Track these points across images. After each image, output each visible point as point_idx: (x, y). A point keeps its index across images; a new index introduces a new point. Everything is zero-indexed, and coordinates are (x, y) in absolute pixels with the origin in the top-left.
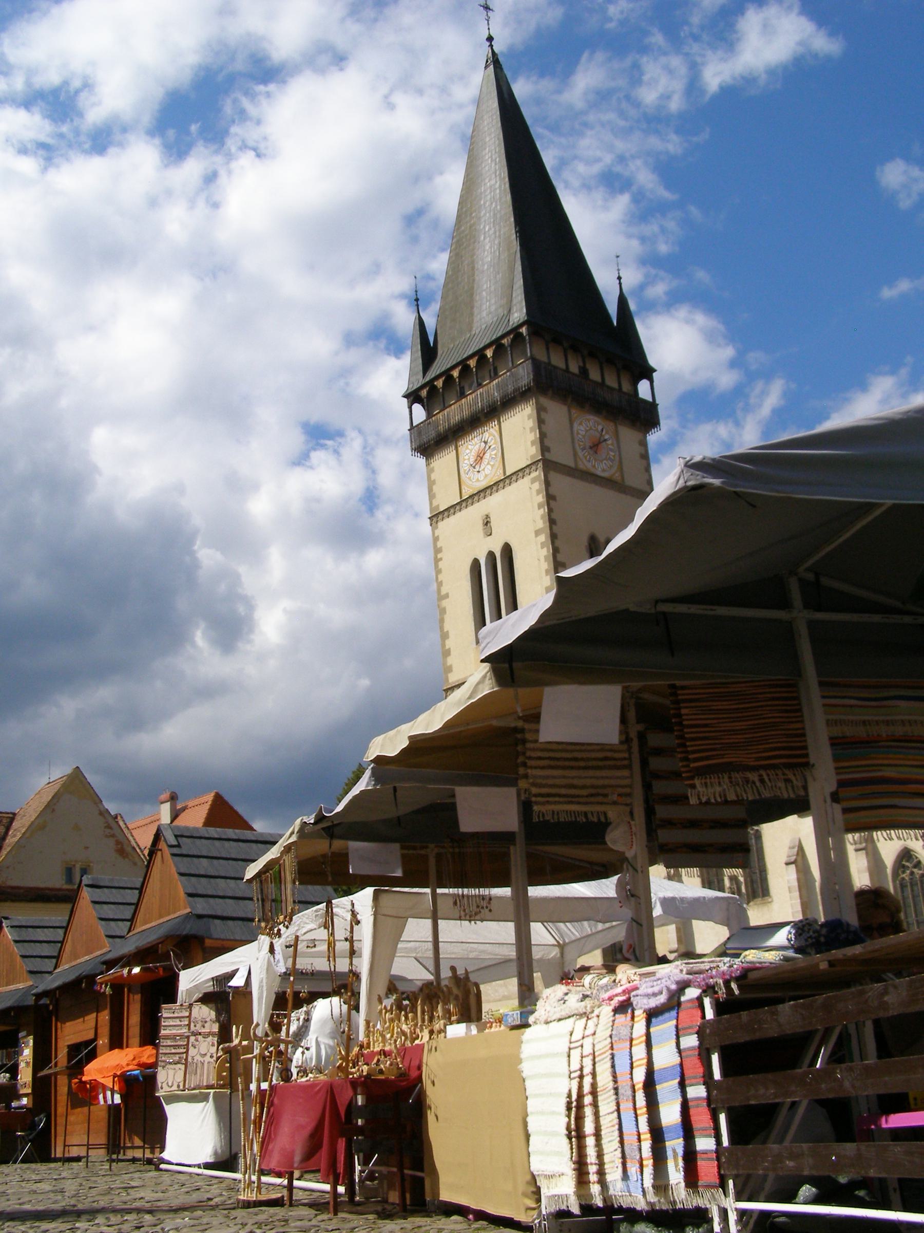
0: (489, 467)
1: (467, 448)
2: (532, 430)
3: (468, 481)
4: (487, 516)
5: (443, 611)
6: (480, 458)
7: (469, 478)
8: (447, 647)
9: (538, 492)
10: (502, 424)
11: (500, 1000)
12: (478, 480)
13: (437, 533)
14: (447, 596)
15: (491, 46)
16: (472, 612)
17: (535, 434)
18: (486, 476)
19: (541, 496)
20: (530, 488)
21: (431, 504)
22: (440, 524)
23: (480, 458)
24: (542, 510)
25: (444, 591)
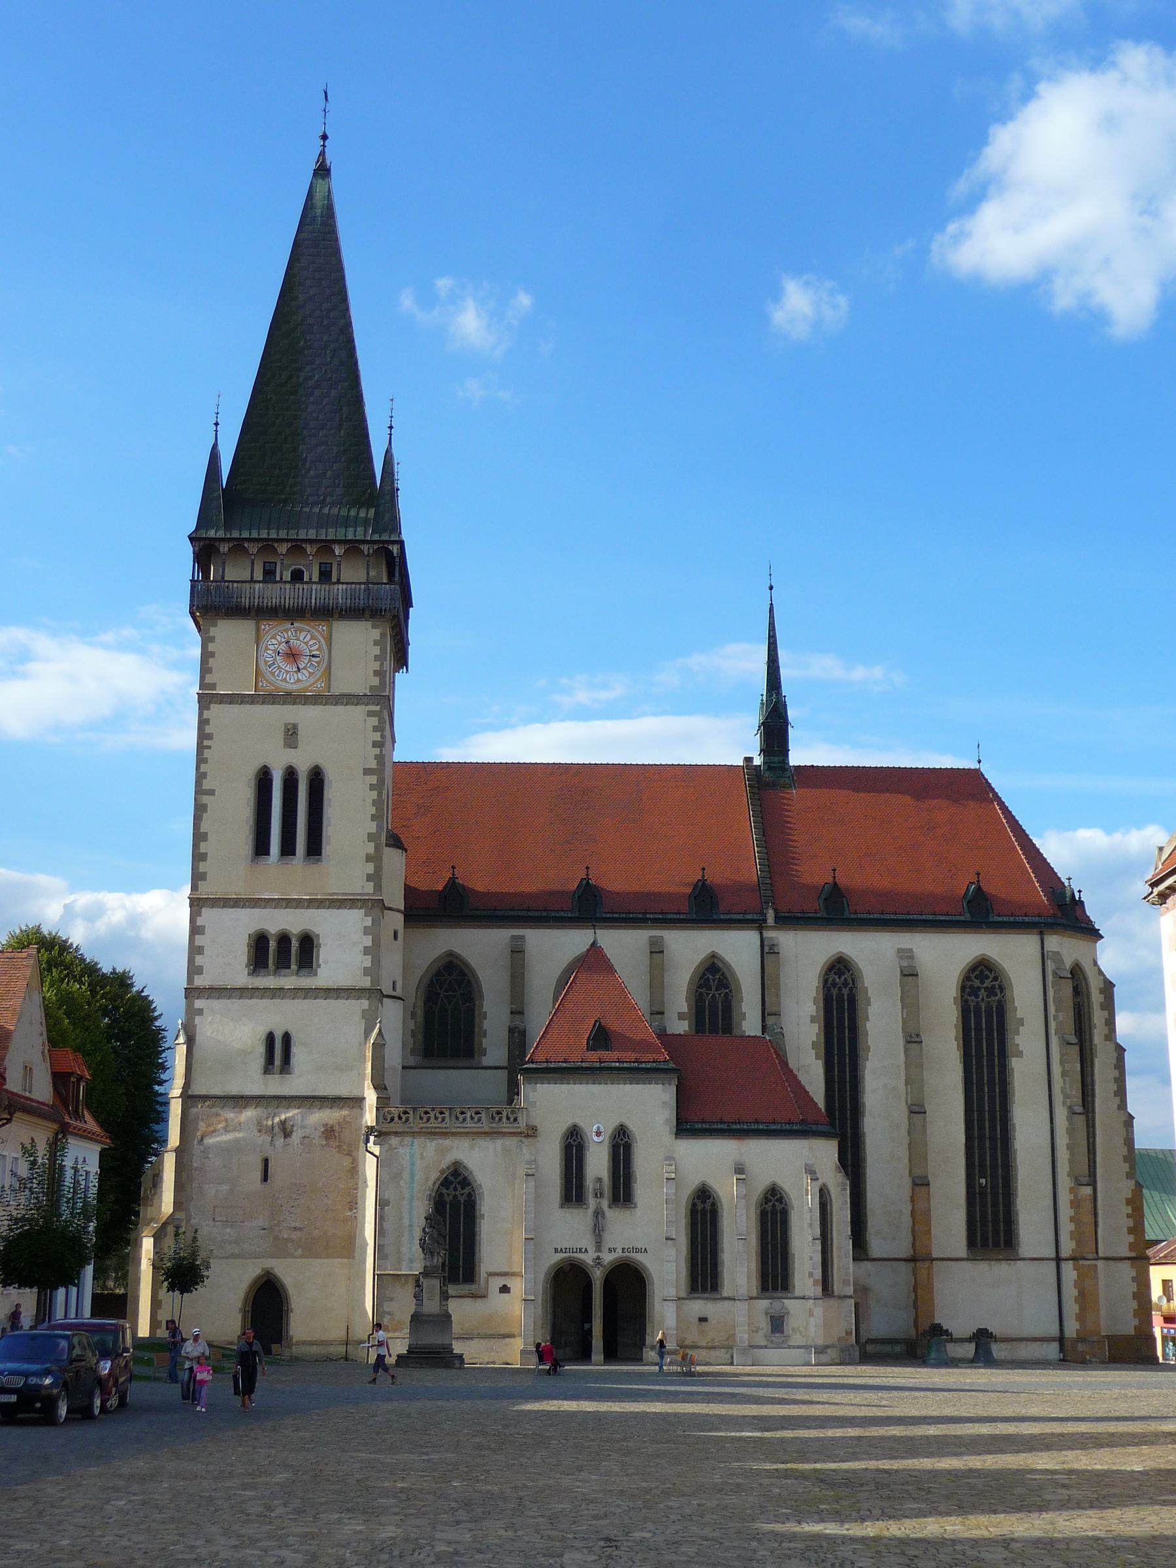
1: (274, 637)
3: (268, 674)
4: (295, 726)
7: (273, 674)
8: (202, 850)
9: (375, 729)
11: (226, 1258)
12: (285, 680)
13: (206, 714)
14: (211, 792)
15: (324, 146)
16: (251, 822)
17: (382, 665)
18: (299, 680)
19: (379, 734)
20: (365, 720)
21: (202, 678)
22: (215, 708)
24: (377, 751)
25: (206, 785)
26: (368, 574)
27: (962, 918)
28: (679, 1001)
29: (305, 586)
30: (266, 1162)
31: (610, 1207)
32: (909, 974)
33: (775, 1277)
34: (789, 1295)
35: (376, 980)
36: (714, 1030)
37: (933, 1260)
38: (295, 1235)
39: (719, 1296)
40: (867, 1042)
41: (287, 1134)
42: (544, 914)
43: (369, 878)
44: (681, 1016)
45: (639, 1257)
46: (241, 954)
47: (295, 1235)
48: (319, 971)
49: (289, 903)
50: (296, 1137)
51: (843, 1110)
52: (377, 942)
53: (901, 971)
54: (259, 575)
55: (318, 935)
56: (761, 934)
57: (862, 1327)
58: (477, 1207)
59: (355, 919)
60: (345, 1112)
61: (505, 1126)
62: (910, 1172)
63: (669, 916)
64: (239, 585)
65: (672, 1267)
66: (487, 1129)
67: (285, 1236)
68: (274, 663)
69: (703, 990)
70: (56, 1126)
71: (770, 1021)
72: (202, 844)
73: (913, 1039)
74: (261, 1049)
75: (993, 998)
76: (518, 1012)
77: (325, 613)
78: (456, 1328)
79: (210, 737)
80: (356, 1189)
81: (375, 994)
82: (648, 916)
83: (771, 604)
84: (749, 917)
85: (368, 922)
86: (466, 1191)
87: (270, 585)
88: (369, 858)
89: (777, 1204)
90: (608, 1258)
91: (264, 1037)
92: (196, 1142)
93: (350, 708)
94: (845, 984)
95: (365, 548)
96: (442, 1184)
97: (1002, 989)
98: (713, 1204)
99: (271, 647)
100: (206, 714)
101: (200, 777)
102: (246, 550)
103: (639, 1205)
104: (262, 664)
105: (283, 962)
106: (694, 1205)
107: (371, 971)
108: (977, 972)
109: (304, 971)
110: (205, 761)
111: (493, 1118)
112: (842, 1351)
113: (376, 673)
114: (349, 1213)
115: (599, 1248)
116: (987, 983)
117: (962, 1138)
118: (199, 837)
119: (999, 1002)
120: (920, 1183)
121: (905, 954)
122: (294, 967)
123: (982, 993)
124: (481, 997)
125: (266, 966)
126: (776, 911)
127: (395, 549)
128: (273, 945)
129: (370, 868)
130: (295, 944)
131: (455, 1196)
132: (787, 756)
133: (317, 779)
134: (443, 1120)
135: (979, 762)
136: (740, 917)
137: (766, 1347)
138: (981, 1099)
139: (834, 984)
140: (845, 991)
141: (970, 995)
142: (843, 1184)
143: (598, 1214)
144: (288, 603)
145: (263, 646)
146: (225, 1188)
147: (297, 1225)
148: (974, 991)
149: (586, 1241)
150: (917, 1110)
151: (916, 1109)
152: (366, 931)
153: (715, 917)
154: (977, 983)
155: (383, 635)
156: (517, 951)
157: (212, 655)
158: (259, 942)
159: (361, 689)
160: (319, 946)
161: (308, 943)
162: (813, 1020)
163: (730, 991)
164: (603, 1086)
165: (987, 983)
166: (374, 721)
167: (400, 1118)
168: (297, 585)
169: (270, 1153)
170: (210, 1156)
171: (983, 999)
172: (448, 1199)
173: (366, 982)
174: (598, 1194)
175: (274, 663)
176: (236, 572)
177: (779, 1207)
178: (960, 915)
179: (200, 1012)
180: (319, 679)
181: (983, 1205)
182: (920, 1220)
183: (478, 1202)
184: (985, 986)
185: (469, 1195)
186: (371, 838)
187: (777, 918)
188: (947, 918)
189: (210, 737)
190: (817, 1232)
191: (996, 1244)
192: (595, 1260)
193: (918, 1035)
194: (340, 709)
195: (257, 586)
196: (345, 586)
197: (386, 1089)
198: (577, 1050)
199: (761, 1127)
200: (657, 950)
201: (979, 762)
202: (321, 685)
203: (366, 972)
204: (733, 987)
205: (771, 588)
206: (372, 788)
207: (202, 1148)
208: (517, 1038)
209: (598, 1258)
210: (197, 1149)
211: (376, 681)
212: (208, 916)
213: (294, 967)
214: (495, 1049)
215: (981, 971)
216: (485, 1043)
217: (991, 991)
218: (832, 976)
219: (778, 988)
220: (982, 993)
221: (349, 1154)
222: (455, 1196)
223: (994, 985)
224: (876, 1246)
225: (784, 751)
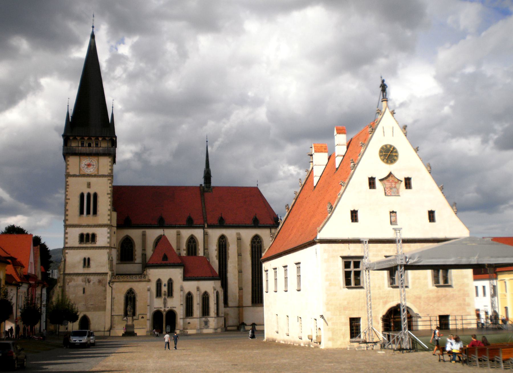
0: (93, 170)
1: (84, 160)
2: (110, 166)
5: (66, 204)
6: (89, 165)
9: (110, 183)
10: (99, 160)
12: (87, 171)
13: (67, 180)
14: (69, 199)
17: (111, 168)
18: (90, 171)
21: (66, 171)
23: (89, 165)
24: (110, 189)
25: (68, 197)
26: (108, 145)
27: (252, 225)
28: (184, 246)
29: (92, 148)
30: (84, 289)
31: (167, 297)
32: (239, 239)
33: (206, 313)
34: (209, 317)
35: (110, 244)
36: (192, 255)
37: (243, 307)
38: (91, 306)
39: (192, 317)
40: (228, 255)
41: (89, 282)
42: (151, 225)
43: (109, 220)
44: (184, 250)
45: (174, 309)
46: (77, 239)
47: (91, 306)
48: (97, 243)
49: (88, 226)
50: (91, 283)
51: (223, 271)
52: (111, 235)
53: (237, 238)
54: (80, 145)
55: (96, 234)
56: (204, 229)
57: (227, 323)
58: (136, 298)
59: (105, 230)
60: (103, 276)
61: (143, 279)
62: (238, 286)
63: (181, 226)
64: (75, 147)
65: (182, 311)
66: (138, 280)
67: (89, 306)
68: (84, 167)
69: (190, 243)
70: (42, 285)
71: (206, 251)
72: (67, 212)
73: (239, 255)
74: (82, 262)
75: (259, 244)
76: (144, 250)
77: (97, 155)
78: (135, 327)
79: (68, 185)
80: (106, 295)
81: (110, 248)
82: (176, 226)
83: (207, 146)
84: (201, 225)
85: (109, 231)
86: (133, 295)
87: (83, 148)
88: (109, 215)
89: (207, 296)
90: (167, 309)
91: (83, 258)
92: (67, 284)
93: (104, 178)
94: (224, 241)
95: (107, 138)
96: (127, 293)
97: (261, 242)
98: (192, 296)
99: (83, 163)
100: (67, 180)
101: (66, 195)
102: (77, 139)
103: (174, 297)
104: (81, 168)
105: (87, 241)
106: (187, 296)
107: (109, 243)
108: (255, 238)
109: (93, 243)
110: (67, 191)
111: (140, 277)
112: (221, 329)
113: (110, 169)
114: (105, 301)
115: (165, 307)
116: (258, 240)
117: (251, 278)
118: (66, 210)
119: (260, 245)
120: (241, 289)
121: (238, 234)
122: (90, 242)
123: (256, 243)
124: (135, 246)
125: (83, 241)
126: (207, 224)
127: (114, 139)
128: (85, 236)
129: (109, 217)
130: (90, 236)
131: (131, 296)
132: (211, 184)
133: (95, 195)
134: (128, 278)
135: (257, 185)
136: (199, 226)
137: (203, 329)
138: (255, 268)
139: (221, 241)
140: (224, 243)
141: (253, 243)
142: (222, 291)
143: (165, 299)
144: (88, 152)
145: (81, 163)
146: (74, 295)
147: (92, 303)
148: (254, 242)
149: (162, 306)
150: (240, 272)
151: (240, 271)
152: (108, 233)
153: (193, 226)
154: (255, 240)
155: (111, 160)
156: (144, 235)
157: (68, 165)
158: (82, 236)
159: (106, 174)
160: (96, 237)
161: (94, 236)
162: (216, 250)
163: (196, 243)
164: (166, 269)
165: (258, 240)
166: (110, 181)
167: (117, 278)
168: (90, 148)
169: (85, 287)
170: (70, 288)
171: (256, 244)
172: (129, 297)
173: (108, 245)
174: (165, 295)
175: (84, 167)
176: (74, 144)
177: (207, 296)
178: (251, 224)
179: (67, 253)
180: (95, 171)
181: (256, 293)
182: (241, 298)
183: (136, 297)
184: (257, 241)
185: (134, 296)
186: (109, 210)
187: (208, 226)
188: (248, 225)
189: (68, 185)
190: (216, 302)
191: (258, 302)
192: (164, 310)
193: (241, 254)
194: (101, 178)
195: (80, 148)
196: (102, 148)
197: (113, 271)
198: (160, 261)
199: (203, 278)
200: (178, 234)
201: (257, 185)
202: (96, 173)
203: (108, 243)
204: (197, 242)
205: (207, 142)
206: (109, 198)
207: (68, 286)
208: (144, 255)
209: (165, 310)
210: (67, 286)
211: (110, 171)
212: (69, 230)
213: (90, 242)
214: (138, 259)
215: (256, 238)
216: (136, 257)
217: (258, 242)
218: (221, 239)
219: (207, 242)
220: (256, 243)
221: (104, 287)
222: (131, 296)
223: (259, 241)
224: (230, 304)
225: (210, 183)
